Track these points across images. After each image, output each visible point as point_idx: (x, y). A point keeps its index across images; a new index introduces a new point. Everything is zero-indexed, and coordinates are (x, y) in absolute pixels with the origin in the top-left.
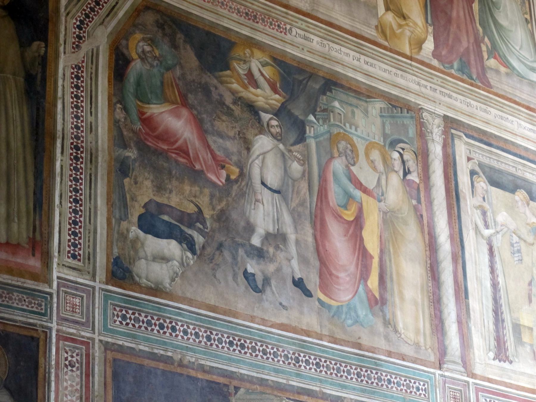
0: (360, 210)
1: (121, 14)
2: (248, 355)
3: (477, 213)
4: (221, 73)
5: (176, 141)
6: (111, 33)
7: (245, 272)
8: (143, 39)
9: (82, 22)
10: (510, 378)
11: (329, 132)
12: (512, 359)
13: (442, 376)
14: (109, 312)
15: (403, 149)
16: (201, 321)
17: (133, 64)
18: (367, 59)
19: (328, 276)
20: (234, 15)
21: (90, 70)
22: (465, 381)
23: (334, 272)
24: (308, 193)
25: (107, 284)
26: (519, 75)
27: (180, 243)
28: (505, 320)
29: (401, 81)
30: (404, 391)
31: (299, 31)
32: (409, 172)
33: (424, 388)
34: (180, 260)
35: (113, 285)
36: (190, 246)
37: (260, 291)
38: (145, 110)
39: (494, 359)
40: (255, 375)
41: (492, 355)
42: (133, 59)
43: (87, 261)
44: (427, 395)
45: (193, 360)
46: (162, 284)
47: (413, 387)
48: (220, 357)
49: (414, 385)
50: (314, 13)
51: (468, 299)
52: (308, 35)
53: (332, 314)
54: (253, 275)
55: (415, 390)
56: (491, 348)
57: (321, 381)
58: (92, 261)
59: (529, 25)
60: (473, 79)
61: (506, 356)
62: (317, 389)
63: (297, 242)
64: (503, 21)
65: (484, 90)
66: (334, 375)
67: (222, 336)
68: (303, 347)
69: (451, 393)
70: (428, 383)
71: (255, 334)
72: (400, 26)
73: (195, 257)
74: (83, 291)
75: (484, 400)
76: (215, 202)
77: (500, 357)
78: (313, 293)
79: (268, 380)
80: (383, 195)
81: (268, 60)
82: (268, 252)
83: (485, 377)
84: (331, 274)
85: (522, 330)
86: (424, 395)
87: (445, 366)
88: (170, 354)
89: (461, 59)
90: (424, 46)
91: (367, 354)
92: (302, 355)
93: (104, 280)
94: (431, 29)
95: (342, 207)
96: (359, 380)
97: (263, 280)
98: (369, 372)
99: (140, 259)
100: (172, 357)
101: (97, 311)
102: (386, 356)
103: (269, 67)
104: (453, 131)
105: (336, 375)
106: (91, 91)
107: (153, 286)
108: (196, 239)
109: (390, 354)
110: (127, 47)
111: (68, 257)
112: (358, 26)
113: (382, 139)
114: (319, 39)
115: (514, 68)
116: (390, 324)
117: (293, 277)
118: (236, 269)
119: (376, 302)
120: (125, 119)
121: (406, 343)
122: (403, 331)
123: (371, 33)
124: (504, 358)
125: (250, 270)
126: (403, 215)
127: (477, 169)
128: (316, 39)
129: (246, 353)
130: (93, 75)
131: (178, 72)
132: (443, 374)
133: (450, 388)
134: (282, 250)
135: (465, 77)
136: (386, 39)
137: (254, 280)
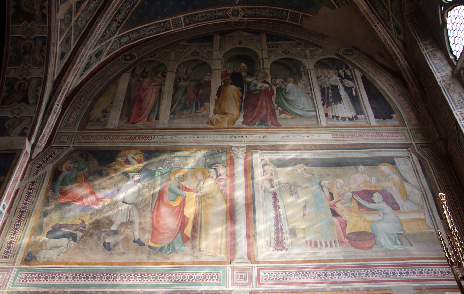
0: (184, 200)
1: (61, 157)
2: (97, 281)
3: (266, 183)
4: (110, 164)
5: (77, 197)
6: (55, 165)
7: (104, 244)
8: (71, 163)
9: (40, 165)
10: (286, 258)
11: (170, 171)
12: (287, 248)
13: (231, 267)
14: (18, 278)
15: (217, 167)
16: (71, 270)
17: (63, 173)
18: (199, 136)
19: (158, 234)
20: (124, 140)
21: (40, 181)
22: (249, 267)
23: (162, 231)
24: (151, 199)
25: (21, 264)
26: (300, 115)
27: (68, 238)
28: (284, 229)
29: (219, 139)
30: (201, 280)
31: (158, 136)
32: (220, 175)
33: (216, 276)
34: (66, 246)
35: (24, 265)
36: (74, 238)
37: (112, 250)
38: (63, 189)
39: (273, 251)
40: (99, 290)
41: (272, 249)
42: (63, 171)
43: (12, 257)
44: (218, 279)
45: (61, 290)
46: (51, 258)
47: (208, 277)
48: (79, 285)
49: (210, 276)
50: (171, 127)
51: (256, 224)
52: (163, 136)
53: (156, 252)
54: (109, 243)
55: (209, 278)
56: (272, 245)
57: (144, 285)
58: (15, 257)
59: (310, 95)
60: (269, 126)
61: (283, 247)
62: (139, 290)
63: (140, 223)
64: (290, 97)
65: (275, 128)
66: (153, 281)
67: (83, 275)
68: (134, 271)
69: (238, 275)
70: (220, 273)
71: (103, 270)
72: (222, 118)
73: (76, 242)
74: (6, 271)
75: (264, 274)
76: (93, 216)
77: (279, 248)
78: (145, 244)
79: (124, 291)
80: (200, 189)
81: (139, 152)
82: (120, 231)
83: (265, 262)
84: (159, 233)
85: (297, 231)
86: (217, 280)
87: (235, 261)
88: (47, 290)
89: (261, 120)
90: (236, 122)
91: (177, 266)
92: (132, 275)
93: (20, 264)
94: (242, 114)
95: (172, 201)
96: (170, 280)
97: (115, 244)
98: (177, 275)
99: (42, 250)
100: (48, 291)
101: (11, 278)
102: (190, 264)
103: (139, 155)
104: (252, 151)
105: (154, 281)
106: (38, 189)
107: (46, 260)
108: (78, 235)
109: (194, 263)
110: (61, 168)
111: (2, 258)
112: (196, 125)
113: (204, 166)
114: (171, 136)
115: (297, 114)
116: (196, 248)
117: (134, 239)
118: (99, 243)
119: (188, 239)
120: (52, 195)
121: (207, 255)
122: (205, 250)
123: (205, 125)
124: (281, 248)
125: (107, 241)
126: (213, 195)
127: (269, 163)
128: (168, 137)
129: (96, 280)
130: (41, 183)
131: (86, 170)
132: (233, 266)
133: (237, 272)
134: (129, 228)
135: (263, 126)
136: (213, 125)
137: (109, 245)
